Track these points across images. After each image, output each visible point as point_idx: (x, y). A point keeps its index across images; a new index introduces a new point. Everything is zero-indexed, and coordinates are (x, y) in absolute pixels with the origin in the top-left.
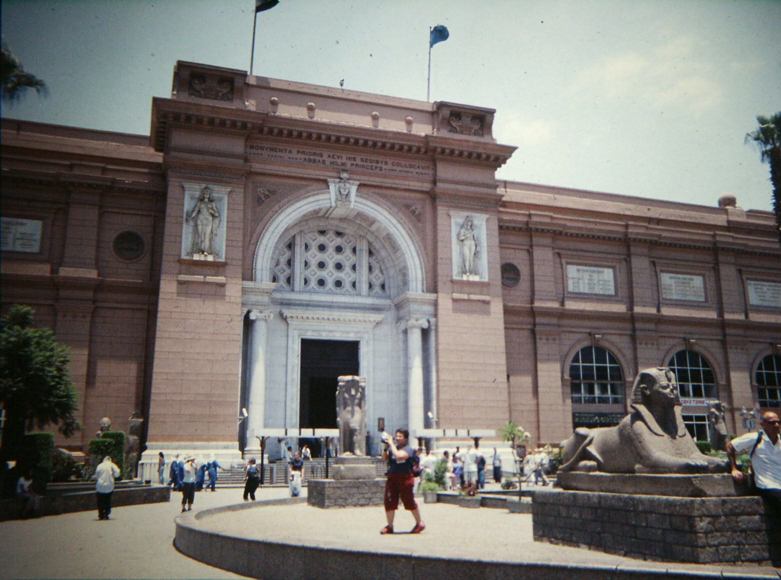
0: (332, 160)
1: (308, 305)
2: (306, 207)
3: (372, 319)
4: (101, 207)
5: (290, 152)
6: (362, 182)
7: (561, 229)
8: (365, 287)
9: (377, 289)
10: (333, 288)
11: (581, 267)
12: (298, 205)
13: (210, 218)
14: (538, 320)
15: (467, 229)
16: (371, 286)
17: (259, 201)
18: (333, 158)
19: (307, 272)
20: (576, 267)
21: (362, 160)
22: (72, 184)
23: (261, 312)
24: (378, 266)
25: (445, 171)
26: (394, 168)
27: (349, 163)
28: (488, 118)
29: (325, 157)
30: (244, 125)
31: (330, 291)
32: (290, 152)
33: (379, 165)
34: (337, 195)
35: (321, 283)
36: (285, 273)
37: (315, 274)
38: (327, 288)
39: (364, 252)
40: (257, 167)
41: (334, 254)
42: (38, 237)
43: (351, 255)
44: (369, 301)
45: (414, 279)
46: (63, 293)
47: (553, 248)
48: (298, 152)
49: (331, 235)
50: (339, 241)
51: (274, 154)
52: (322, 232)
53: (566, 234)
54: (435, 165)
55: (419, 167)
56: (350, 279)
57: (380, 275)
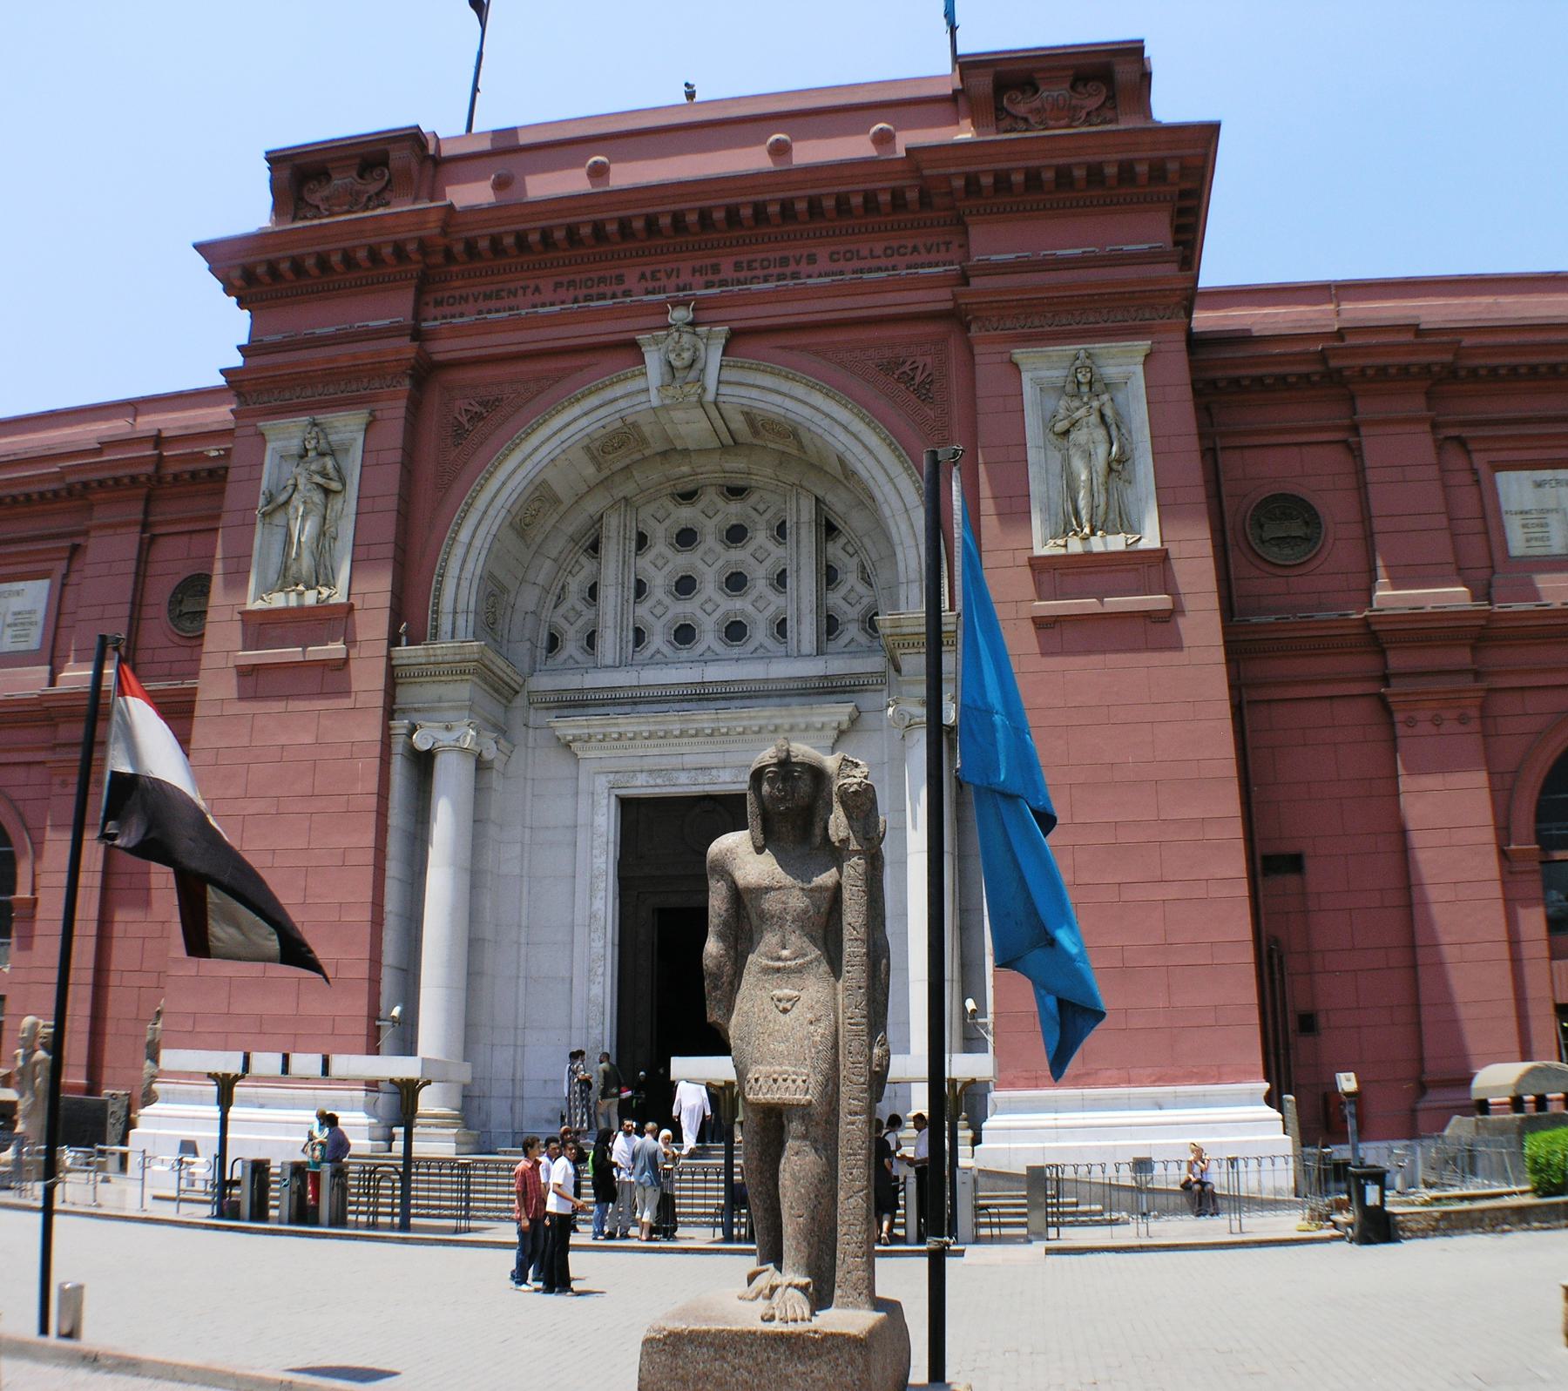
0: (650, 285)
1: (634, 700)
2: (583, 422)
3: (817, 721)
4: (145, 526)
5: (537, 289)
6: (736, 325)
7: (1448, 358)
9: (852, 631)
10: (718, 647)
11: (1547, 474)
12: (557, 422)
13: (318, 497)
14: (1396, 661)
15: (1077, 395)
16: (830, 626)
17: (459, 433)
18: (654, 278)
19: (643, 610)
21: (738, 266)
23: (448, 728)
24: (853, 563)
25: (996, 243)
26: (841, 265)
28: (1124, 72)
29: (631, 280)
30: (399, 251)
31: (708, 655)
32: (537, 289)
33: (788, 270)
34: (678, 379)
35: (685, 634)
36: (580, 623)
37: (662, 612)
38: (700, 647)
39: (804, 532)
40: (443, 349)
41: (719, 548)
42: (39, 617)
43: (771, 546)
44: (813, 668)
47: (1435, 426)
48: (558, 285)
49: (710, 497)
50: (734, 511)
51: (492, 304)
52: (688, 496)
53: (1473, 372)
54: (966, 232)
55: (915, 249)
57: (861, 588)
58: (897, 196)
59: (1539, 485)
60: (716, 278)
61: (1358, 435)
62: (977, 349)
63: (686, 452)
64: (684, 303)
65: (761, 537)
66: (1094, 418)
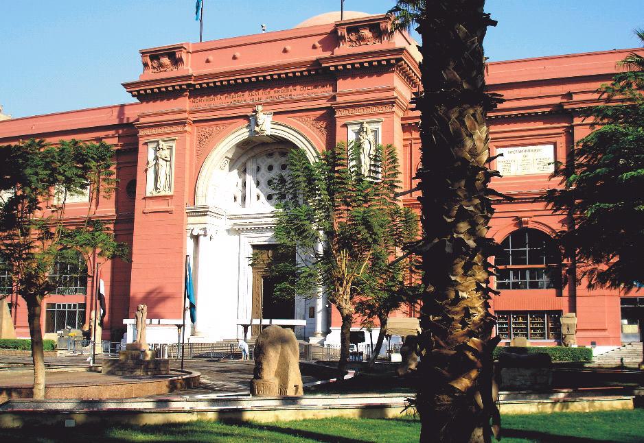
21: (275, 92)
25: (344, 85)
33: (290, 92)
49: (277, 156)
50: (283, 160)
52: (270, 155)
64: (260, 104)
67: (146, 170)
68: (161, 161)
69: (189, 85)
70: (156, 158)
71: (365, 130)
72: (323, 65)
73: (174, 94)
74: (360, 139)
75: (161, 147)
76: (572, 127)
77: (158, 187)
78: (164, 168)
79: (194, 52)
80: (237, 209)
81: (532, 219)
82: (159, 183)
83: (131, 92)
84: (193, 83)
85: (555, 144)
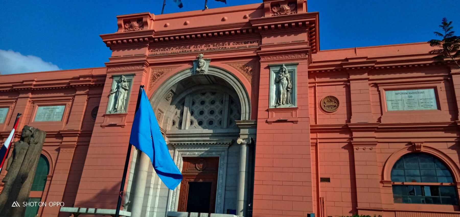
0: (195, 49)
2: (180, 77)
8: (225, 123)
11: (400, 91)
20: (394, 92)
21: (214, 46)
22: (75, 85)
27: (205, 49)
33: (225, 46)
43: (220, 105)
45: (244, 112)
46: (65, 139)
49: (208, 94)
50: (213, 97)
51: (163, 52)
52: (203, 94)
56: (218, 119)
58: (247, 30)
59: (397, 94)
60: (209, 48)
61: (349, 83)
62: (261, 64)
63: (203, 85)
64: (202, 53)
65: (217, 103)
66: (285, 78)
67: (109, 96)
68: (121, 90)
69: (150, 38)
70: (118, 88)
71: (284, 70)
72: (253, 25)
73: (138, 44)
74: (280, 77)
75: (123, 79)
76: (450, 76)
77: (116, 107)
78: (123, 94)
79: (156, 20)
80: (176, 131)
81: (422, 145)
82: (117, 105)
83: (106, 42)
84: (153, 37)
85: (435, 89)
